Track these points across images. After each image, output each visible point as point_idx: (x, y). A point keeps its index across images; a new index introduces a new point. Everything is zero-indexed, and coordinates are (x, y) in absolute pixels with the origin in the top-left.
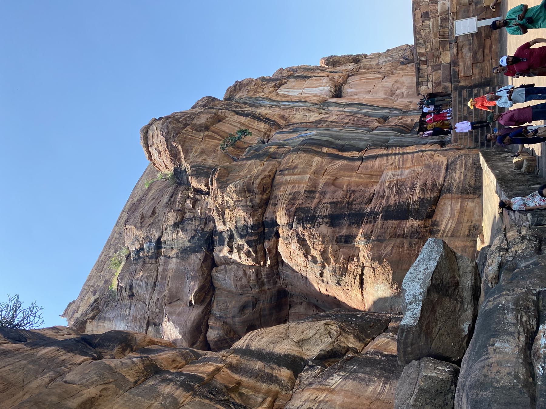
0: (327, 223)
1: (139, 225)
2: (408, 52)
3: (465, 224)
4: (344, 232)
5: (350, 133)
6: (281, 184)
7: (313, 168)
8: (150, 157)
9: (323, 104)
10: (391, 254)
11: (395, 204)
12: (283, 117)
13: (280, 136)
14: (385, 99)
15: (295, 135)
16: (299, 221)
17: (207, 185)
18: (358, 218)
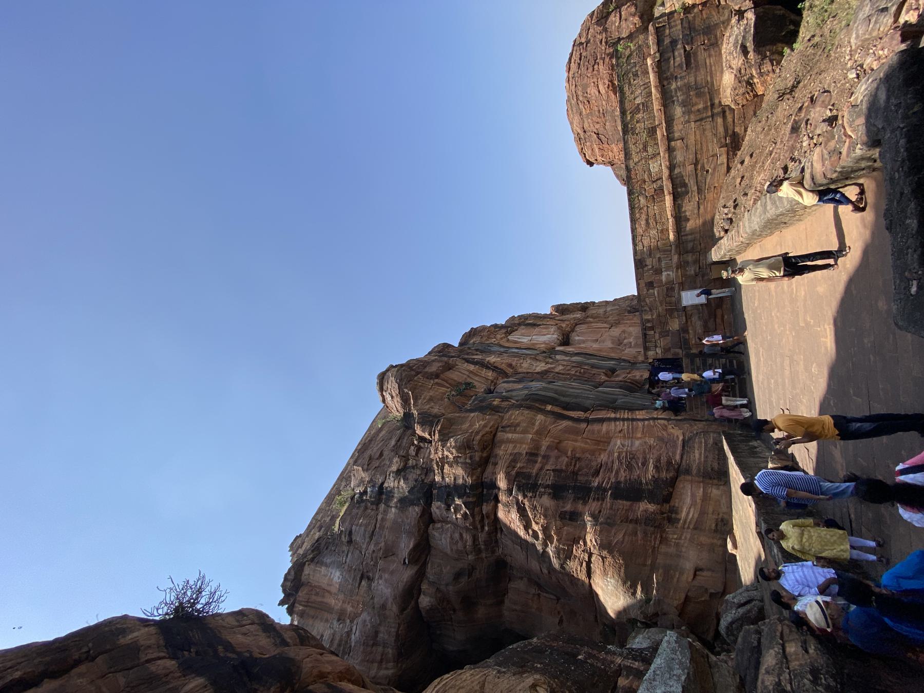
0: (550, 494)
1: (366, 467)
2: (635, 302)
3: (710, 515)
4: (568, 507)
5: (576, 388)
6: (502, 442)
7: (536, 428)
8: (384, 401)
9: (550, 352)
10: (622, 543)
11: (626, 480)
12: (510, 365)
13: (505, 385)
14: (612, 348)
15: (520, 386)
16: (519, 489)
17: (430, 434)
18: (584, 493)
